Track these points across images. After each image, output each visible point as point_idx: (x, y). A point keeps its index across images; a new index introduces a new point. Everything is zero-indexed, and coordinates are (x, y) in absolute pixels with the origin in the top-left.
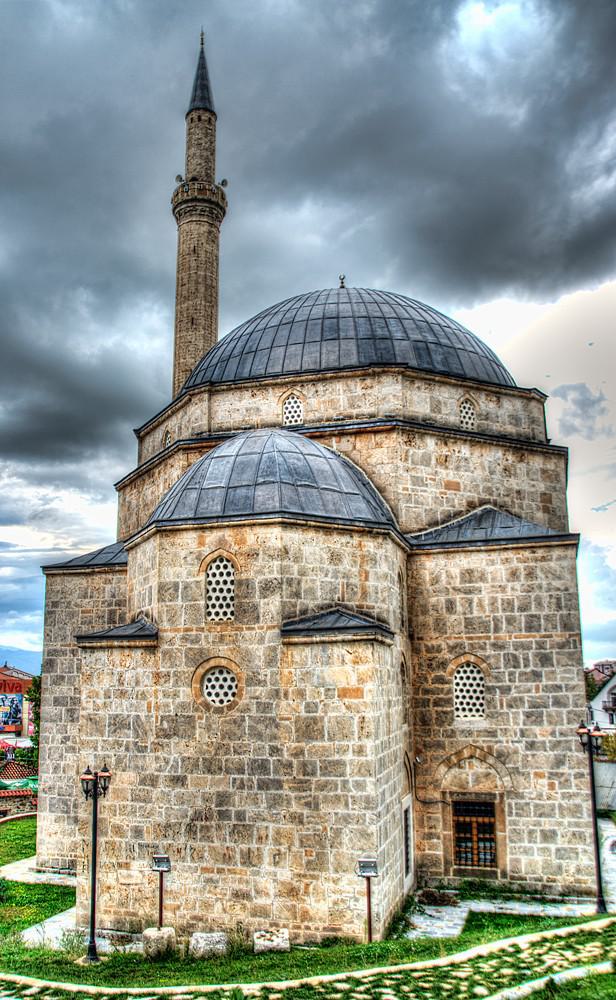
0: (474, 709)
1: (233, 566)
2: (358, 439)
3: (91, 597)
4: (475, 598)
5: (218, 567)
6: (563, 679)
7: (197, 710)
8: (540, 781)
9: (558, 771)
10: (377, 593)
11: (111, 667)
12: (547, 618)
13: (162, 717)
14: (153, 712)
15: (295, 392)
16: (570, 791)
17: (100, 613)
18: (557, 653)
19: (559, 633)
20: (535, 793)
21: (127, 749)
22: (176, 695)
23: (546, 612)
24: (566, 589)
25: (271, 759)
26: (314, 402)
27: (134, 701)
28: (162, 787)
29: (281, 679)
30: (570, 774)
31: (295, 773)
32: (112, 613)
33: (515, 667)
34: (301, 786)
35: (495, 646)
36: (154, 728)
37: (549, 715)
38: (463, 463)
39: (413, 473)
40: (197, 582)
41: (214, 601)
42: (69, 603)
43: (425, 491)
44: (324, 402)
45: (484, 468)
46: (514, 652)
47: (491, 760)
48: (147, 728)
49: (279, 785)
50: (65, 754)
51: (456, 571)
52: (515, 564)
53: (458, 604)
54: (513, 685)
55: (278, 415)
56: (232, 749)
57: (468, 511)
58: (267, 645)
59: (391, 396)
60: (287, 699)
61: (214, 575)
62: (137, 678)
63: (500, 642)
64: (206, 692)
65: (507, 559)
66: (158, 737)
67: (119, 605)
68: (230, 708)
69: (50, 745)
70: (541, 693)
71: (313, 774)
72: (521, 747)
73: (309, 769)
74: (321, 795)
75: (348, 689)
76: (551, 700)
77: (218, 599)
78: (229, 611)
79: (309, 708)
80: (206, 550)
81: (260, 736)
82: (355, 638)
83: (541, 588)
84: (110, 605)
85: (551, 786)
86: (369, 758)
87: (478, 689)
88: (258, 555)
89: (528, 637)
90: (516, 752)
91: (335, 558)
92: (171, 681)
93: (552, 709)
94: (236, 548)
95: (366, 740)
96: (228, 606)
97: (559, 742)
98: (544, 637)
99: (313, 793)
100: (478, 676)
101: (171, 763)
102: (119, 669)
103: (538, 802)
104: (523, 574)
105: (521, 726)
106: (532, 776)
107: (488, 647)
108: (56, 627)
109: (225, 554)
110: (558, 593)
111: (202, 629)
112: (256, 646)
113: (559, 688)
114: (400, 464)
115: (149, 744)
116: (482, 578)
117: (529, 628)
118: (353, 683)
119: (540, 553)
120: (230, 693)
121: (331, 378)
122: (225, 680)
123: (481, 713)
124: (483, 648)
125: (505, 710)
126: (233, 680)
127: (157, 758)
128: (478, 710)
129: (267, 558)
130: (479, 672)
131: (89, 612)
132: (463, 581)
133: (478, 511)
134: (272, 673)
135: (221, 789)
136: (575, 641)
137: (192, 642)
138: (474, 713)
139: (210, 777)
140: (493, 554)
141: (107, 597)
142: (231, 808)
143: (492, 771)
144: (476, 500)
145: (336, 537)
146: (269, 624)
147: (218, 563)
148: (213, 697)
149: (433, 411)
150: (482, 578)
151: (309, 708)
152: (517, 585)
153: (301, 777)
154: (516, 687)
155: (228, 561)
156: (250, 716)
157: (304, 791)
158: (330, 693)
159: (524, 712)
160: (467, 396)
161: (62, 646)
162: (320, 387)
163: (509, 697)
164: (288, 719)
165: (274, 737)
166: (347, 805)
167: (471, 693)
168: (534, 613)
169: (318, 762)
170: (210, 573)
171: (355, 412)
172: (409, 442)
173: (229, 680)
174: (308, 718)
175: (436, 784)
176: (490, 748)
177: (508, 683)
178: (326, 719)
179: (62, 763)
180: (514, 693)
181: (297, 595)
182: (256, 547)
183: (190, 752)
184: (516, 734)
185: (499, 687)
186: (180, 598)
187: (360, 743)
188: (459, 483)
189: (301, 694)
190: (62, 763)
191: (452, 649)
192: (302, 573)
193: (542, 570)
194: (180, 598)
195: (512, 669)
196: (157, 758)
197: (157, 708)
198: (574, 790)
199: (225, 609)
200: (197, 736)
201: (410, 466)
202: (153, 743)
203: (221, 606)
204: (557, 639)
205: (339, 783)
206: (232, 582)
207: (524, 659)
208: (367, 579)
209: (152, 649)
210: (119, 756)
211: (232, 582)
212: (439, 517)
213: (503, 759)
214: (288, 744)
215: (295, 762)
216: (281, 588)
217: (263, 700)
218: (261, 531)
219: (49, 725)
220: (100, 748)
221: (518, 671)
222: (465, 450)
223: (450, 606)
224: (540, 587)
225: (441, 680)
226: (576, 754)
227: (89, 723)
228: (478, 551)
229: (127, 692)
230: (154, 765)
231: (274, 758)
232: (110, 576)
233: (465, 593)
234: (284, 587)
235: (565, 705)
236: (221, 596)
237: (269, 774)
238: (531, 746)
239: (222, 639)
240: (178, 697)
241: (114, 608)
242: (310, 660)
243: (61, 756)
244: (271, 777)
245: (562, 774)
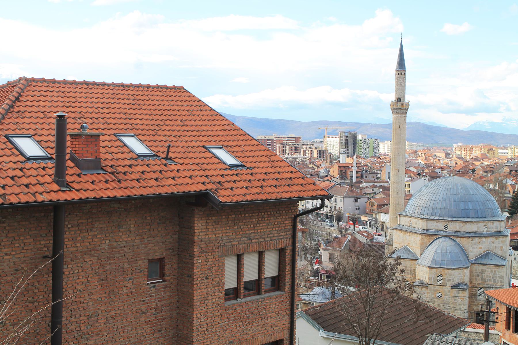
4: (483, 275)
22: (431, 296)
35: (486, 284)
51: (480, 269)
52: (492, 269)
80: (438, 273)
91: (459, 274)
104: (493, 271)
114: (470, 245)
116: (485, 271)
117: (494, 282)
119: (497, 268)
132: (481, 271)
133: (486, 252)
149: (477, 229)
150: (485, 271)
162: (453, 223)
171: (460, 230)
172: (472, 240)
175: (473, 309)
181: (453, 281)
191: (478, 284)
192: (454, 278)
201: (472, 245)
209: (427, 288)
212: (477, 255)
223: (478, 276)
225: (475, 290)
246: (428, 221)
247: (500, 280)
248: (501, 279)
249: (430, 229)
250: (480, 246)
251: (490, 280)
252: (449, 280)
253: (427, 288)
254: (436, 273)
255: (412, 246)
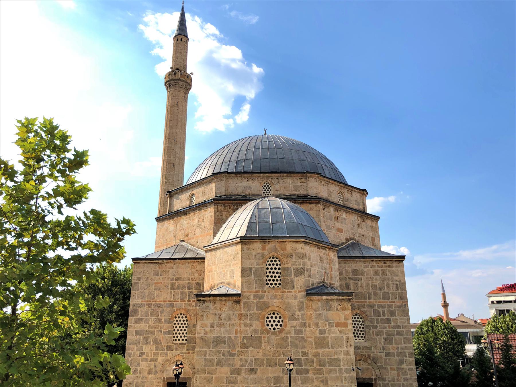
0: (360, 336)
1: (279, 261)
2: (302, 205)
3: (161, 275)
4: (359, 283)
5: (272, 261)
6: (400, 322)
7: (262, 333)
8: (393, 372)
9: (401, 367)
10: (335, 278)
11: (214, 311)
12: (392, 294)
13: (243, 337)
14: (238, 335)
15: (268, 181)
16: (407, 377)
17: (166, 284)
18: (398, 310)
19: (398, 301)
20: (391, 378)
21: (224, 355)
22: (251, 325)
23: (392, 291)
24: (400, 281)
25: (303, 358)
26: (277, 186)
27: (228, 329)
28: (243, 374)
29: (306, 317)
30: (406, 369)
31: (315, 365)
32: (172, 284)
33: (379, 316)
34: (318, 372)
35: (368, 305)
36: (239, 343)
37: (395, 340)
38: (343, 221)
39: (326, 223)
40: (262, 268)
41: (270, 278)
42: (147, 278)
43: (331, 232)
44: (282, 187)
45: (351, 224)
46: (378, 309)
47: (369, 361)
48: (235, 343)
49: (307, 371)
50: (141, 363)
51: (350, 270)
52: (377, 268)
53: (351, 285)
54: (378, 325)
55: (260, 191)
56: (282, 353)
57: (346, 243)
58: (298, 300)
59: (314, 187)
60: (310, 327)
61: (270, 265)
62: (229, 317)
63: (371, 304)
64: (266, 324)
65: (373, 265)
66: (241, 348)
67: (177, 280)
68: (281, 332)
69: (132, 358)
70: (391, 329)
71: (324, 365)
72: (383, 355)
73: (322, 363)
74: (329, 376)
75: (340, 323)
76: (396, 332)
77: (272, 277)
78: (278, 283)
79: (322, 332)
80: (266, 252)
81: (296, 346)
82: (343, 298)
83: (389, 279)
84: (172, 280)
85: (398, 375)
86: (352, 357)
87: (362, 327)
88: (292, 256)
89: (384, 302)
90: (381, 357)
91: (321, 260)
92: (249, 318)
93: (397, 337)
94: (281, 252)
95: (350, 348)
96: (277, 280)
97: (401, 353)
98: (391, 302)
99: (325, 375)
100: (361, 320)
101: (249, 361)
102: (219, 312)
103: (393, 382)
105: (383, 345)
106: (389, 369)
107: (366, 306)
108: (139, 291)
109: (276, 255)
110: (397, 282)
111: (265, 292)
112: (293, 301)
113: (399, 327)
115: (236, 352)
116: (362, 274)
117: (384, 298)
118: (343, 320)
119: (388, 263)
120: (279, 324)
121: (286, 176)
122: (276, 318)
123: (363, 338)
124: (364, 307)
125: (375, 337)
126: (280, 318)
127: (241, 359)
128: (362, 337)
129: (297, 258)
130: (361, 318)
131: (159, 283)
132: (353, 275)
134: (302, 314)
135: (276, 375)
136: (405, 305)
137: (260, 298)
138: (360, 338)
139: (270, 368)
140: (366, 263)
141: (170, 276)
142: (282, 385)
143: (370, 367)
144: (349, 238)
145: (321, 250)
146: (300, 290)
147: (271, 259)
148: (270, 326)
150: (362, 274)
151: (322, 332)
152: (378, 278)
153: (319, 367)
154: (380, 326)
155: (277, 258)
156: (291, 337)
157: (320, 374)
158: (331, 324)
159: (383, 338)
160: (340, 190)
161: (141, 301)
163: (377, 330)
164: (311, 338)
165: (304, 347)
166: (342, 381)
167: (358, 328)
168: (386, 291)
169: (327, 359)
170: (268, 263)
171: (297, 193)
172: (324, 209)
173: (278, 317)
174: (320, 337)
176: (369, 355)
177: (376, 324)
178: (330, 338)
179: (139, 368)
180: (378, 329)
181: (310, 276)
182: (291, 252)
183: (260, 356)
184: (380, 349)
185: (372, 326)
186: (253, 275)
187: (347, 349)
188: (342, 230)
189: (317, 325)
190: (139, 368)
193: (389, 272)
194: (253, 275)
195: (377, 317)
196: (241, 359)
197: (241, 332)
198: (409, 376)
199: (275, 282)
200: (263, 347)
202: (238, 351)
203: (273, 280)
204: (397, 304)
205: (338, 370)
206: (279, 269)
207: (383, 312)
208: (332, 271)
209: (238, 302)
210: (219, 359)
211: (279, 269)
213: (375, 361)
214: (311, 351)
215: (315, 359)
216: (304, 272)
217: (298, 328)
218: (295, 245)
219: (131, 346)
220: (207, 355)
221: (380, 318)
222: (344, 215)
224: (388, 279)
226: (409, 358)
227: (201, 341)
228: (360, 261)
229: (223, 324)
230: (239, 363)
231: (304, 358)
232: (172, 265)
233: (354, 280)
234: (306, 272)
235: (402, 335)
236: (274, 275)
237: (302, 366)
238: (388, 354)
239: (275, 297)
240: (253, 326)
241: (174, 281)
242: (320, 308)
243: (138, 364)
244: (303, 367)
245: (403, 368)
246: (230, 180)
247: (397, 292)
248: (400, 291)
249: (233, 194)
250: (338, 225)
251: (376, 294)
252: (299, 272)
253: (238, 302)
254: (263, 256)
255: (193, 238)
